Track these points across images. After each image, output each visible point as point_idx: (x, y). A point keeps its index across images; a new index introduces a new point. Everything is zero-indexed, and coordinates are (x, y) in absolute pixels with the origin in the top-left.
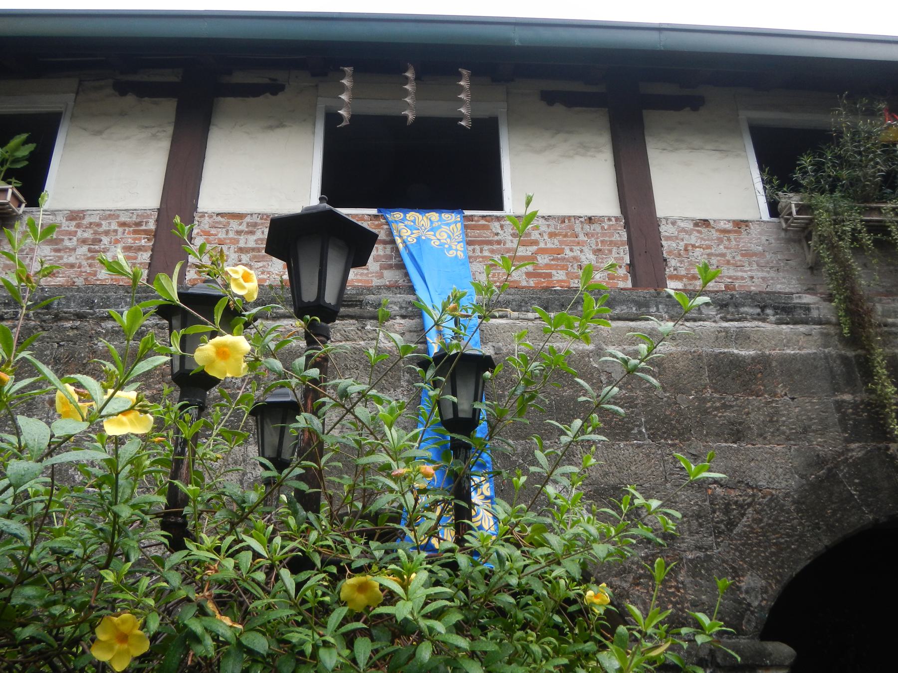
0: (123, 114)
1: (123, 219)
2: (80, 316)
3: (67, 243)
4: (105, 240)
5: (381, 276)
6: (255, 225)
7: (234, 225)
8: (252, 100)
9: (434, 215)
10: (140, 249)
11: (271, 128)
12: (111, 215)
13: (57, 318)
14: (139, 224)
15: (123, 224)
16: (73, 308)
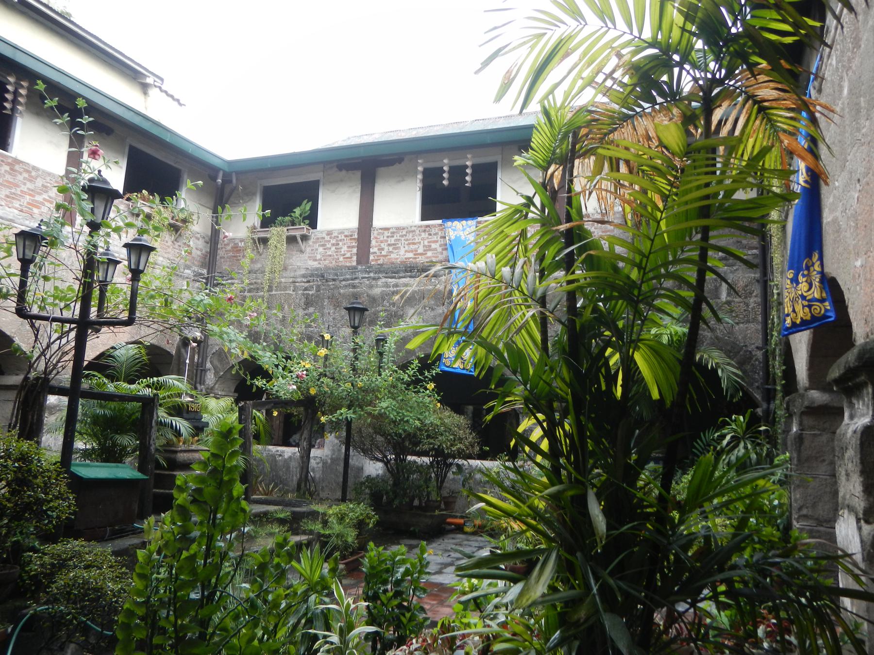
0: (342, 181)
1: (346, 233)
2: (334, 280)
3: (328, 246)
4: (341, 243)
5: (442, 253)
6: (393, 233)
7: (386, 233)
8: (391, 168)
9: (464, 222)
10: (353, 247)
11: (399, 182)
12: (341, 232)
13: (327, 281)
14: (351, 236)
15: (346, 236)
16: (331, 277)
